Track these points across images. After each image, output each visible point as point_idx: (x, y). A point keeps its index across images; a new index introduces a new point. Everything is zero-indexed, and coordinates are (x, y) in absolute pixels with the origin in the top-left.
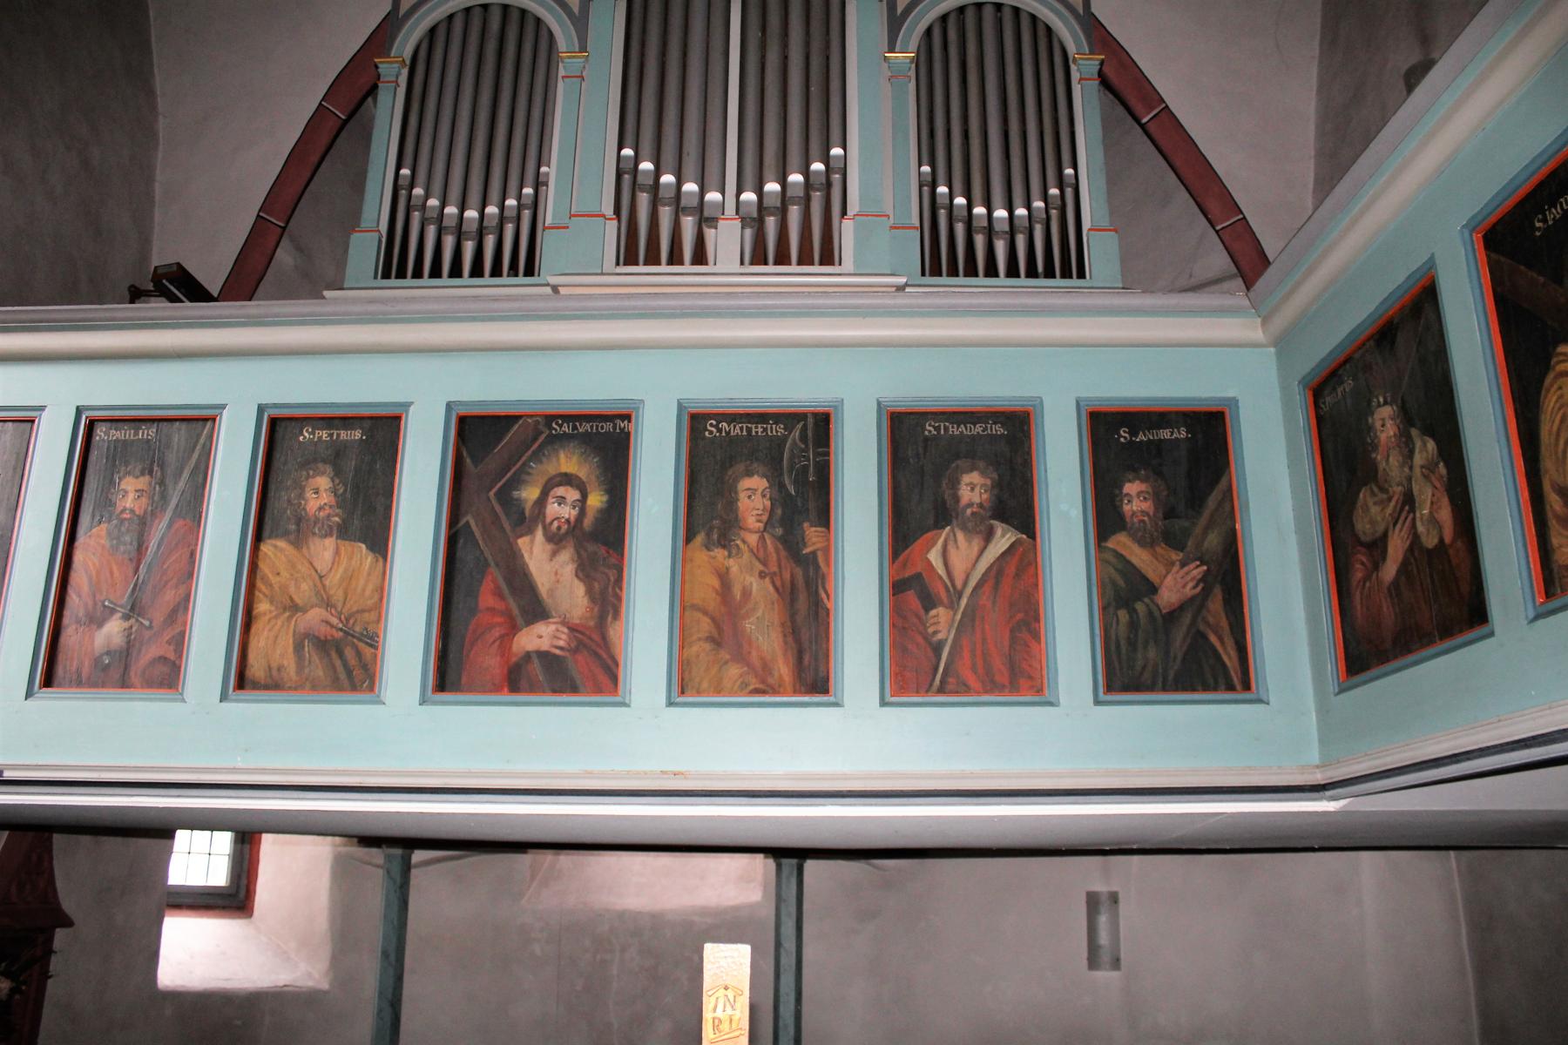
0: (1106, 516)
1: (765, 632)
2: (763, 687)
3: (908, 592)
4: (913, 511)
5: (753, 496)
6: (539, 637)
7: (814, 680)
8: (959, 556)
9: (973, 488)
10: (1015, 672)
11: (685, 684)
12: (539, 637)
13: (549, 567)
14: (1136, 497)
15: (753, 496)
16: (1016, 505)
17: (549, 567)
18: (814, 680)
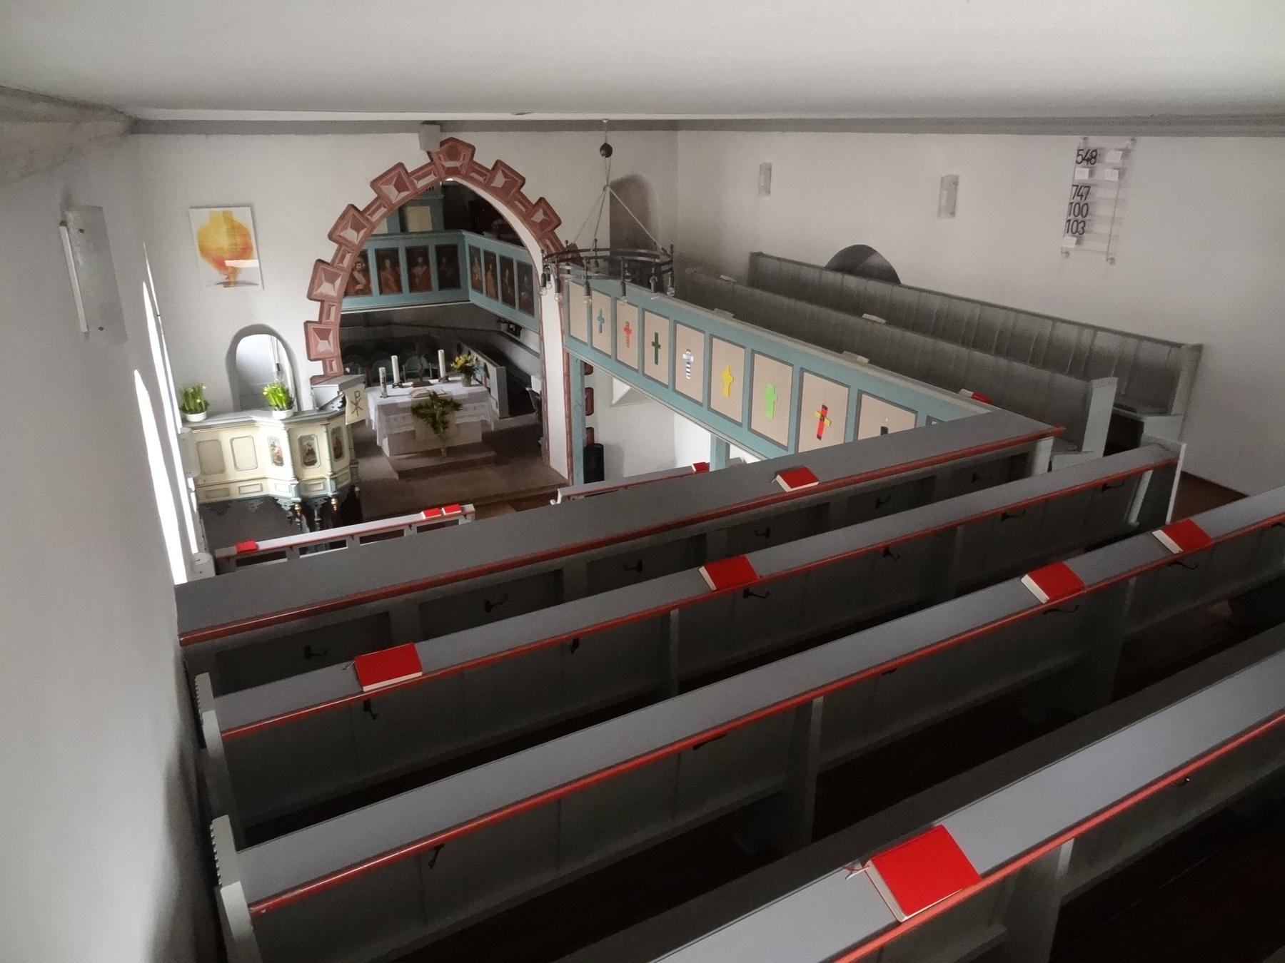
0: (439, 263)
1: (392, 284)
2: (393, 292)
3: (411, 277)
4: (411, 264)
5: (388, 263)
6: (359, 287)
7: (400, 290)
8: (419, 270)
9: (420, 260)
10: (427, 287)
11: (381, 292)
12: (359, 287)
13: (359, 276)
14: (444, 260)
15: (388, 263)
16: (426, 262)
17: (359, 276)
18: (400, 290)
